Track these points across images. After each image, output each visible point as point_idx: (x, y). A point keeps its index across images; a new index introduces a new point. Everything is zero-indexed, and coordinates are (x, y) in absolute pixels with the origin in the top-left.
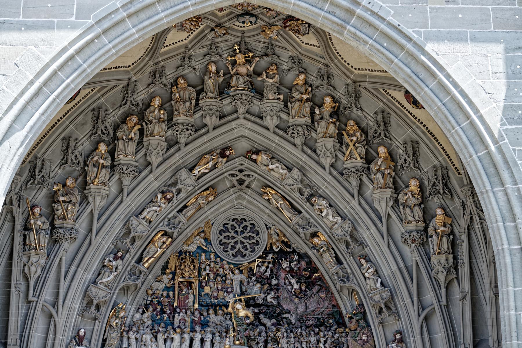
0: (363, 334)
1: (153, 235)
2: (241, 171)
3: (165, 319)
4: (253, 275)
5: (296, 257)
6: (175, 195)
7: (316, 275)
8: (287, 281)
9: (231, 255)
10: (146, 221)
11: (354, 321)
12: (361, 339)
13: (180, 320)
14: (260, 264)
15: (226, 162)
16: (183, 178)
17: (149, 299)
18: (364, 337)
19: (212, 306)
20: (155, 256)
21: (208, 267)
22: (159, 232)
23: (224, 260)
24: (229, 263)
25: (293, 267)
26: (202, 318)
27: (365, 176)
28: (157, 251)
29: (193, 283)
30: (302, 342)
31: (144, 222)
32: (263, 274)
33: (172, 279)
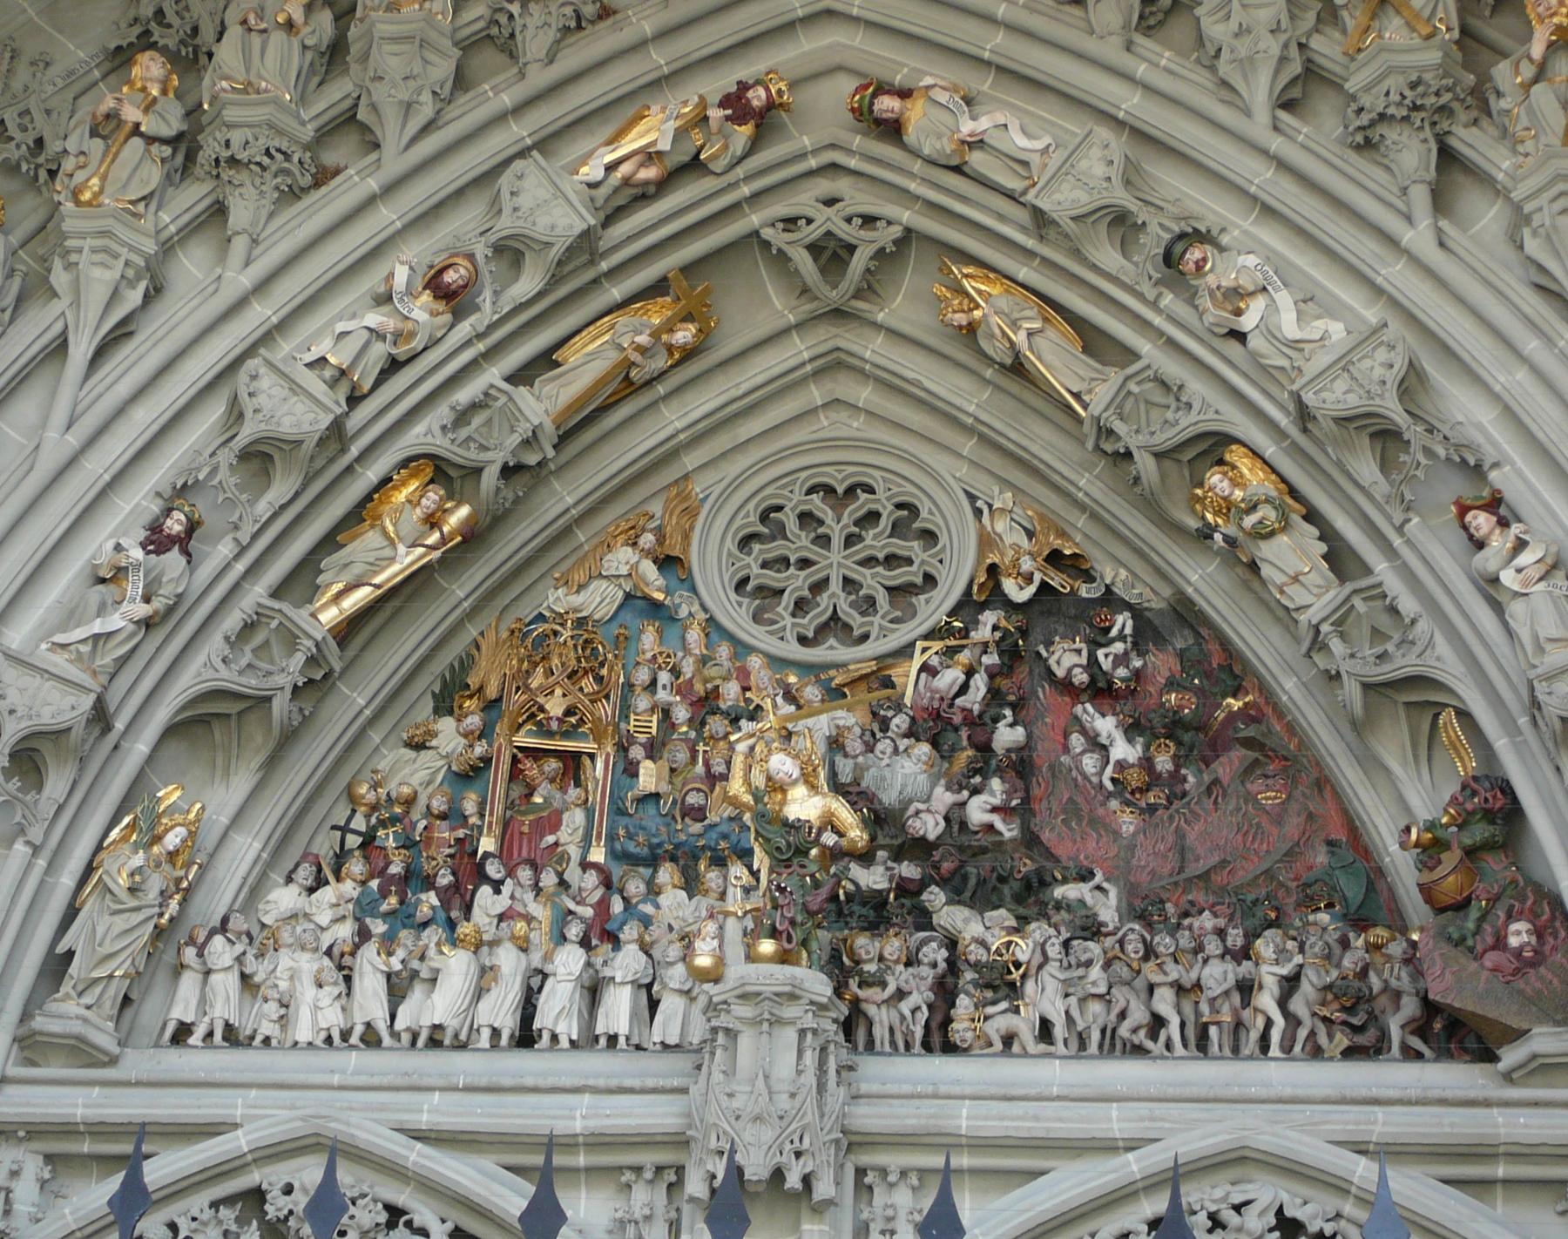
0: (1510, 917)
1: (372, 474)
2: (830, 202)
3: (424, 911)
4: (899, 707)
5: (1123, 622)
6: (486, 278)
7: (1235, 704)
8: (1077, 741)
9: (791, 636)
10: (333, 384)
11: (1450, 859)
12: (1500, 943)
13: (501, 917)
14: (935, 661)
15: (754, 146)
16: (525, 201)
17: (359, 823)
18: (1519, 934)
19: (673, 859)
20: (377, 580)
21: (664, 677)
22: (405, 463)
23: (752, 649)
24: (778, 663)
25: (1106, 664)
26: (617, 906)
27: (1463, 116)
28: (392, 560)
29: (592, 757)
30: (1151, 989)
31: (314, 383)
32: (951, 706)
33: (480, 738)
